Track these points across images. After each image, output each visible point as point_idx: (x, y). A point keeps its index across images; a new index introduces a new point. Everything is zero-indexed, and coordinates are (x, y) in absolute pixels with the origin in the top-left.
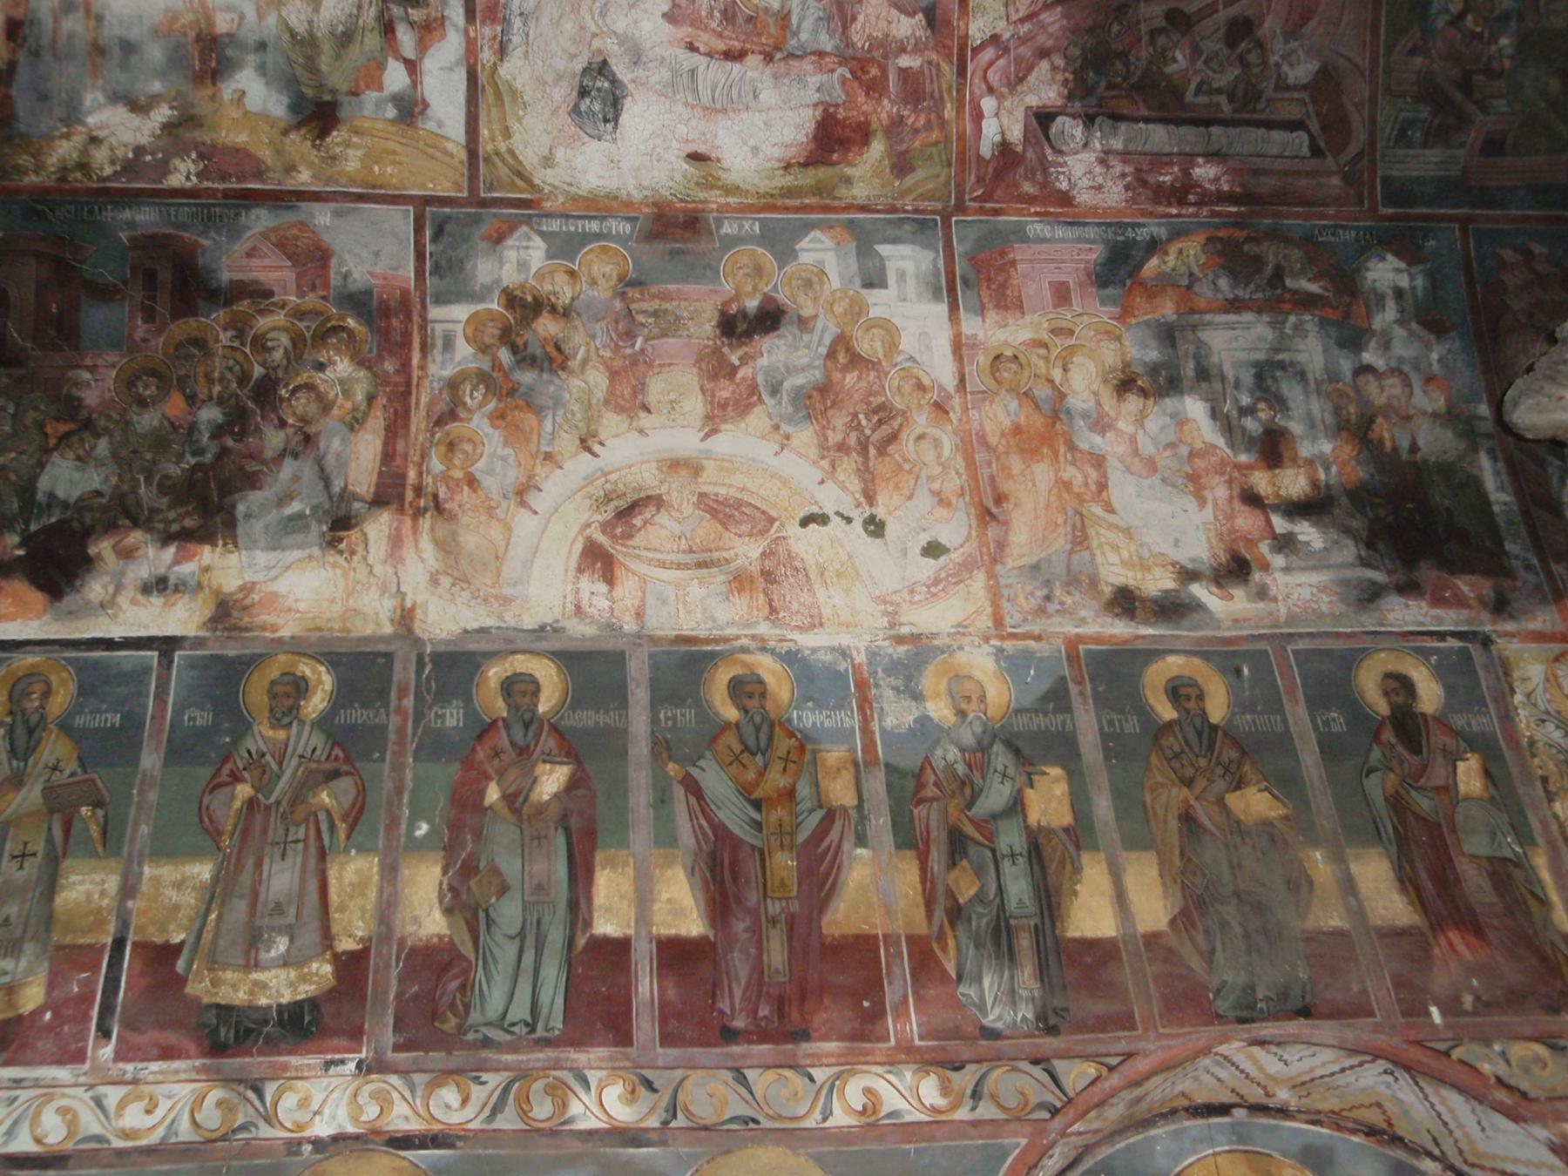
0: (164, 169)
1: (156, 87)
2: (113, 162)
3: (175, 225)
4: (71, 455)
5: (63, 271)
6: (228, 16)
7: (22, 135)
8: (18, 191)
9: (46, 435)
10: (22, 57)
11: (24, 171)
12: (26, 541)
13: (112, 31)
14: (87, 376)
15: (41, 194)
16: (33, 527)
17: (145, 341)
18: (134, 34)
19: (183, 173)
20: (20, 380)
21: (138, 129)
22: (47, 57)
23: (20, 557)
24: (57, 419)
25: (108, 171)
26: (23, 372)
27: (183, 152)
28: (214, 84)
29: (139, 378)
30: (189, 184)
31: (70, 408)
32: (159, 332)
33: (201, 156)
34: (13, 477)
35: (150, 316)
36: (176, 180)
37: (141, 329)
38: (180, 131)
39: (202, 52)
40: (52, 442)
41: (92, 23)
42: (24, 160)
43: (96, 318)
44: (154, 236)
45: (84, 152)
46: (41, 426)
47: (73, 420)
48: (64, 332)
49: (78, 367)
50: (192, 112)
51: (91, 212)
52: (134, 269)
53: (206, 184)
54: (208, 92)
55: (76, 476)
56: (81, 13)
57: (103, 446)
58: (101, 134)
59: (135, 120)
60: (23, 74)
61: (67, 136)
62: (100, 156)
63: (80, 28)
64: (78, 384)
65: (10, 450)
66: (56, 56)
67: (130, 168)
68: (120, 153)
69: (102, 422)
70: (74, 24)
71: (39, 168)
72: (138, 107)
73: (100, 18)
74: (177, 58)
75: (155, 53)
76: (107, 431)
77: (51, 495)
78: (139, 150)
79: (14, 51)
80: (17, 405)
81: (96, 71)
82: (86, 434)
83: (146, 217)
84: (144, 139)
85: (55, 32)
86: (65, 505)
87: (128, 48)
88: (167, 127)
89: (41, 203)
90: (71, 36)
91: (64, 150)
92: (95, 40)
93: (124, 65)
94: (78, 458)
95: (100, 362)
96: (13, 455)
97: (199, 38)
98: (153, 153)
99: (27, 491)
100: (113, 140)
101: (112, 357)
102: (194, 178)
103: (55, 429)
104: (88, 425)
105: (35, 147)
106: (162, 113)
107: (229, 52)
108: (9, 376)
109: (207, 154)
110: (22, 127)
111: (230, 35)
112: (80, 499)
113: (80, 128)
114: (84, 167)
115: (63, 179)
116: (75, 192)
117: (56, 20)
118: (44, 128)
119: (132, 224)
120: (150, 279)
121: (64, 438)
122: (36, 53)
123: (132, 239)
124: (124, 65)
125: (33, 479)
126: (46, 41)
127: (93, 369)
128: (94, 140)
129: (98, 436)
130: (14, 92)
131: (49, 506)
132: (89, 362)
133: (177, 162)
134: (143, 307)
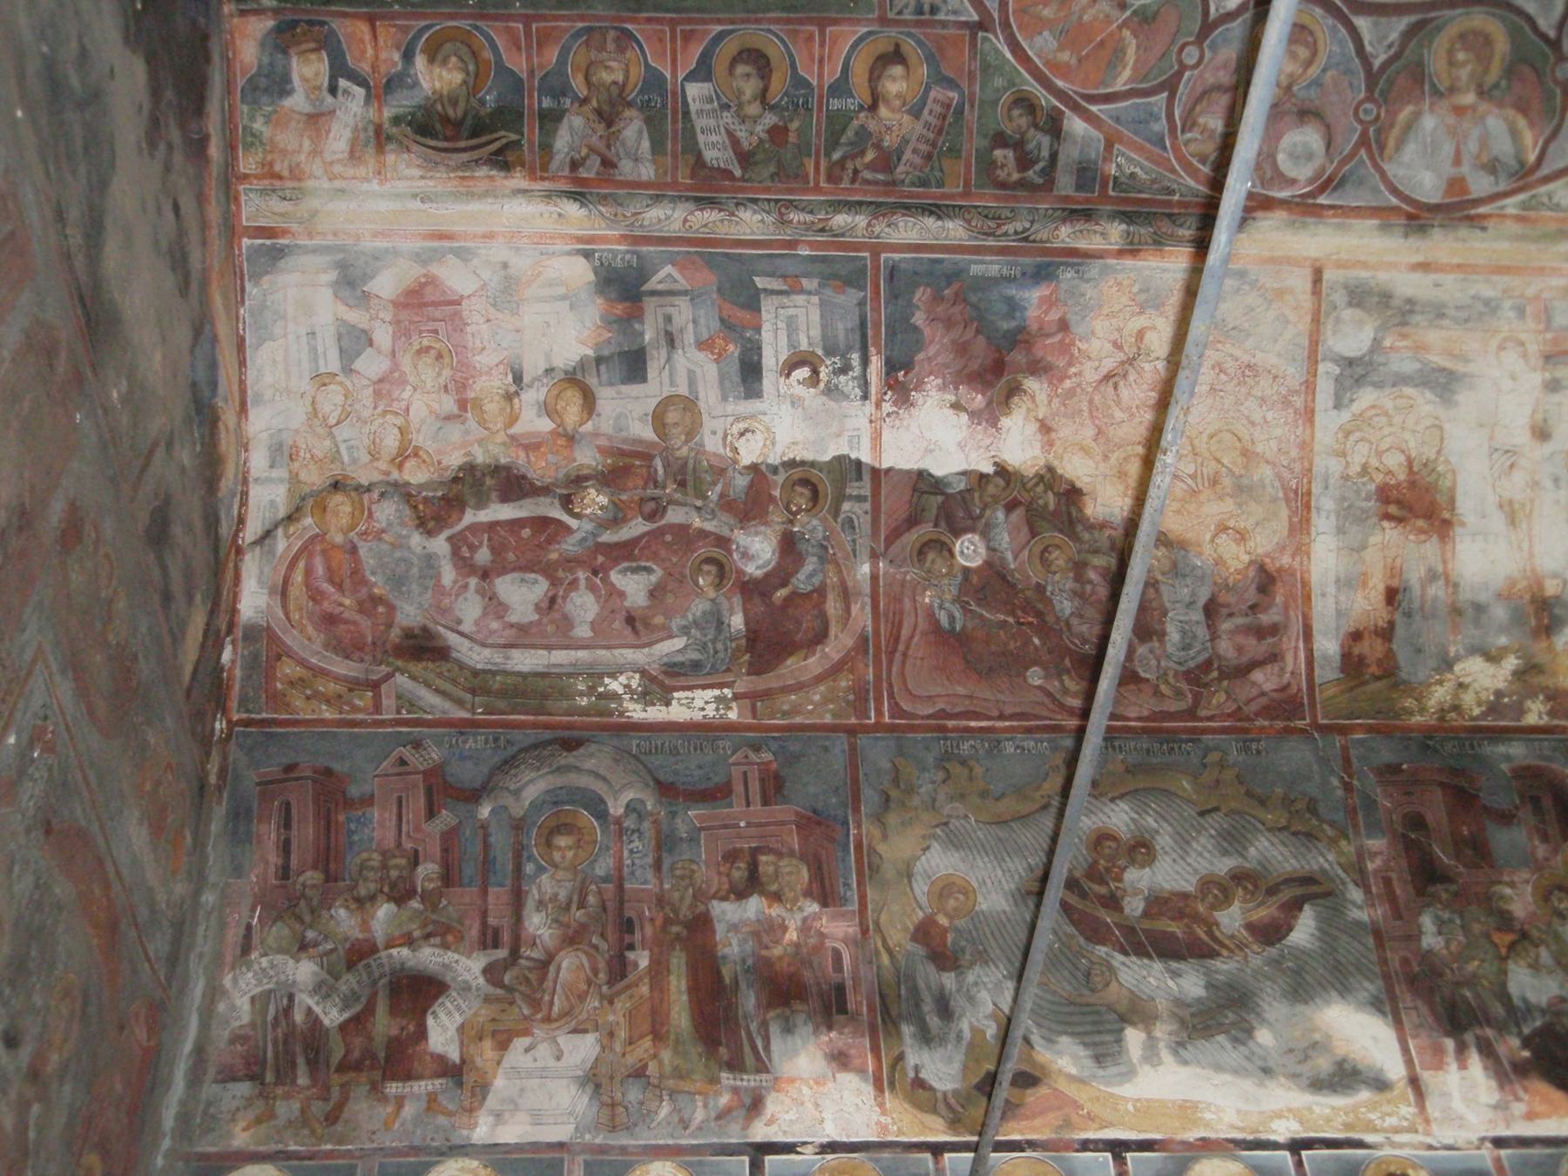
0: (1521, 711)
1: (1503, 640)
2: (1479, 705)
3: (1545, 758)
4: (1522, 963)
5: (1463, 798)
6: (1555, 582)
7: (1404, 682)
8: (1409, 729)
9: (1496, 945)
10: (1398, 617)
11: (1411, 713)
12: (1527, 1042)
13: (1465, 595)
14: (1508, 891)
15: (1428, 733)
16: (1526, 1031)
17: (1547, 859)
18: (1483, 597)
19: (1536, 712)
20: (1456, 894)
21: (1494, 676)
22: (1418, 618)
23: (1526, 1060)
24: (1499, 929)
25: (1476, 712)
26: (1454, 888)
27: (1533, 695)
28: (1548, 637)
29: (1551, 893)
30: (1542, 722)
31: (1505, 921)
32: (1556, 851)
33: (1548, 698)
34: (1485, 983)
35: (1545, 838)
36: (1531, 719)
37: (1541, 851)
38: (1527, 677)
39: (1536, 613)
40: (1504, 951)
41: (1450, 590)
42: (1409, 703)
43: (1504, 839)
44: (1528, 768)
45: (1456, 696)
46: (1488, 936)
47: (1510, 930)
48: (1478, 852)
49: (1500, 882)
50: (1536, 660)
51: (1472, 747)
52: (1522, 796)
53: (1556, 722)
54: (1544, 644)
55: (1535, 982)
56: (1441, 582)
57: (1544, 955)
58: (1467, 680)
59: (1490, 669)
60: (1400, 632)
61: (1440, 683)
62: (1468, 699)
63: (1441, 594)
64: (1502, 897)
65: (1473, 959)
66: (1425, 618)
67: (1493, 709)
68: (1484, 696)
69: (1535, 933)
70: (1437, 590)
71: (1422, 710)
72: (1492, 657)
73: (1456, 585)
74: (1517, 618)
75: (1500, 613)
76: (1542, 942)
77: (1525, 1000)
78: (1499, 694)
79: (1392, 613)
80: (1462, 917)
81: (1455, 629)
82: (1526, 943)
83: (1517, 751)
84: (1501, 685)
85: (1422, 596)
86: (1543, 1012)
87: (1479, 608)
88: (1519, 674)
89: (1428, 740)
90: (1435, 599)
91: (1440, 695)
92: (1453, 603)
93: (1477, 622)
94: (1530, 966)
95: (1516, 879)
96: (1476, 963)
97: (1533, 601)
98: (1510, 696)
99: (1504, 996)
100: (1476, 685)
101: (1525, 875)
102: (1546, 718)
103: (1504, 939)
104: (1524, 935)
105: (1418, 692)
106: (1511, 663)
107: (1557, 611)
108: (1446, 891)
109: (1553, 696)
110: (1403, 675)
111: (1557, 597)
112: (1550, 1005)
113: (1449, 676)
114: (1456, 708)
115: (1442, 719)
116: (1453, 729)
117: (1423, 588)
118: (1421, 676)
119: (1508, 758)
120: (1535, 801)
121: (1512, 947)
122: (1409, 615)
123: (1513, 770)
124: (1477, 622)
125: (1504, 985)
126: (1416, 604)
127: (1512, 885)
128: (1461, 685)
129: (1537, 946)
130: (1394, 647)
131: (1529, 1010)
132: (1506, 878)
133: (1529, 703)
134: (1538, 830)
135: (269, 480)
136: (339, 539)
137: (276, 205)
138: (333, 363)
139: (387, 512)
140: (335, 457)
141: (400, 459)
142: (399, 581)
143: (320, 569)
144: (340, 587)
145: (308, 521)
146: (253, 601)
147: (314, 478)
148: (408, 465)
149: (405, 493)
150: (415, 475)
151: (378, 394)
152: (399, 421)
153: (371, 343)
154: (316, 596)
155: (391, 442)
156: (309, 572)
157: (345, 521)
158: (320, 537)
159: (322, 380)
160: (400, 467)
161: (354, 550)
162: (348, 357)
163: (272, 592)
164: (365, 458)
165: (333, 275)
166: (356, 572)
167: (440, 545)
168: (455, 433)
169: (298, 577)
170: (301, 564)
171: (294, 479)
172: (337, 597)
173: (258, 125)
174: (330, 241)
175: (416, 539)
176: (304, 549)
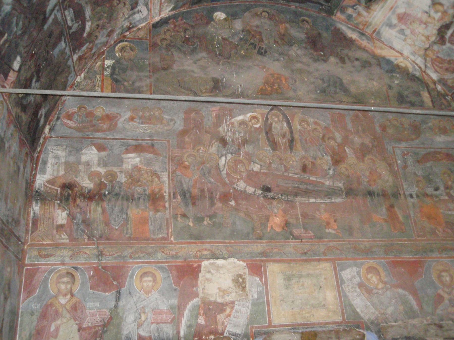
135: (417, 59)
136: (434, 57)
137: (371, 27)
138: (403, 37)
139: (436, 47)
140: (420, 48)
141: (428, 38)
142: (449, 55)
143: (438, 64)
144: (442, 63)
145: (428, 59)
146: (435, 76)
147: (422, 52)
148: (430, 38)
149: (435, 43)
150: (433, 39)
151: (414, 35)
152: (421, 35)
153: (403, 30)
154: (441, 68)
155: (423, 38)
156: (437, 65)
157: (432, 54)
158: (432, 59)
159: (405, 40)
160: (429, 40)
161: (438, 57)
162: (404, 34)
163: (435, 72)
164: (423, 44)
165: (387, 28)
166: (442, 59)
167: (448, 45)
168: (429, 28)
169: (436, 67)
170: (434, 65)
171: (420, 56)
172: (444, 65)
173: (355, 22)
174: (381, 24)
175: (444, 47)
176: (432, 63)
